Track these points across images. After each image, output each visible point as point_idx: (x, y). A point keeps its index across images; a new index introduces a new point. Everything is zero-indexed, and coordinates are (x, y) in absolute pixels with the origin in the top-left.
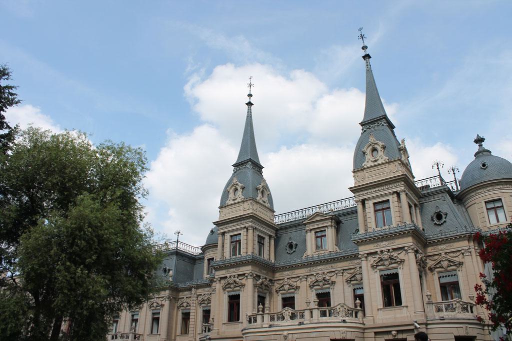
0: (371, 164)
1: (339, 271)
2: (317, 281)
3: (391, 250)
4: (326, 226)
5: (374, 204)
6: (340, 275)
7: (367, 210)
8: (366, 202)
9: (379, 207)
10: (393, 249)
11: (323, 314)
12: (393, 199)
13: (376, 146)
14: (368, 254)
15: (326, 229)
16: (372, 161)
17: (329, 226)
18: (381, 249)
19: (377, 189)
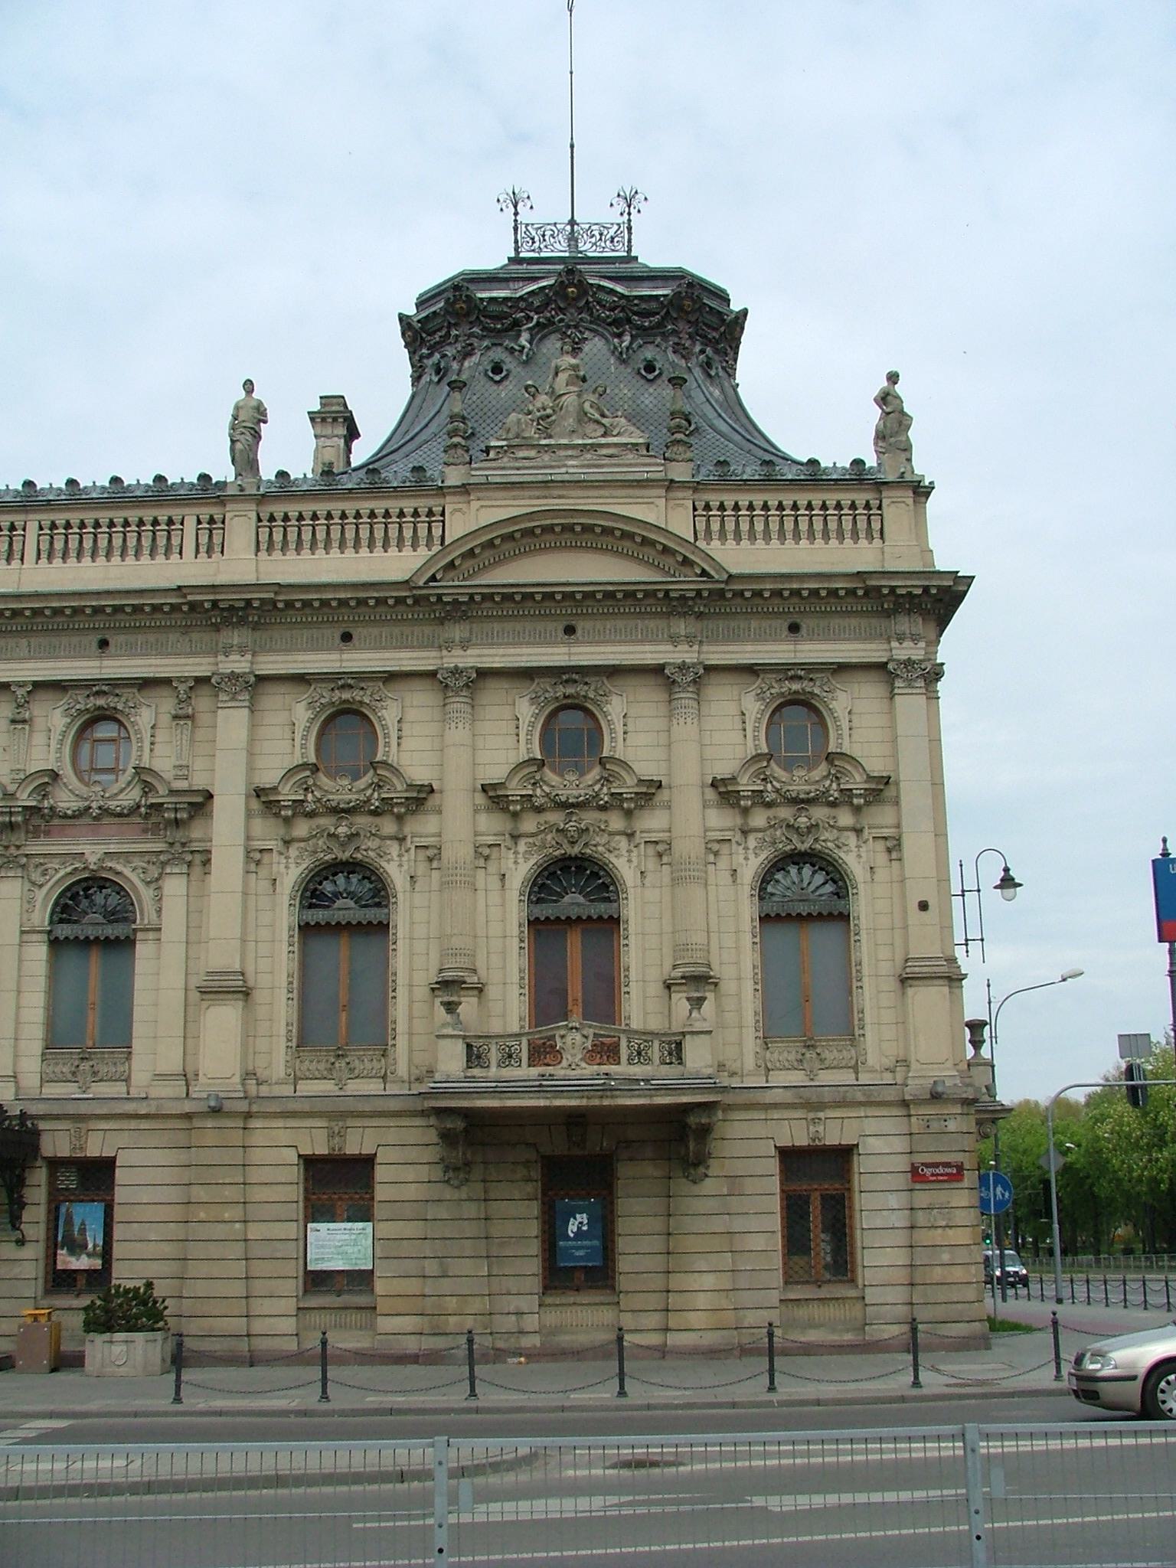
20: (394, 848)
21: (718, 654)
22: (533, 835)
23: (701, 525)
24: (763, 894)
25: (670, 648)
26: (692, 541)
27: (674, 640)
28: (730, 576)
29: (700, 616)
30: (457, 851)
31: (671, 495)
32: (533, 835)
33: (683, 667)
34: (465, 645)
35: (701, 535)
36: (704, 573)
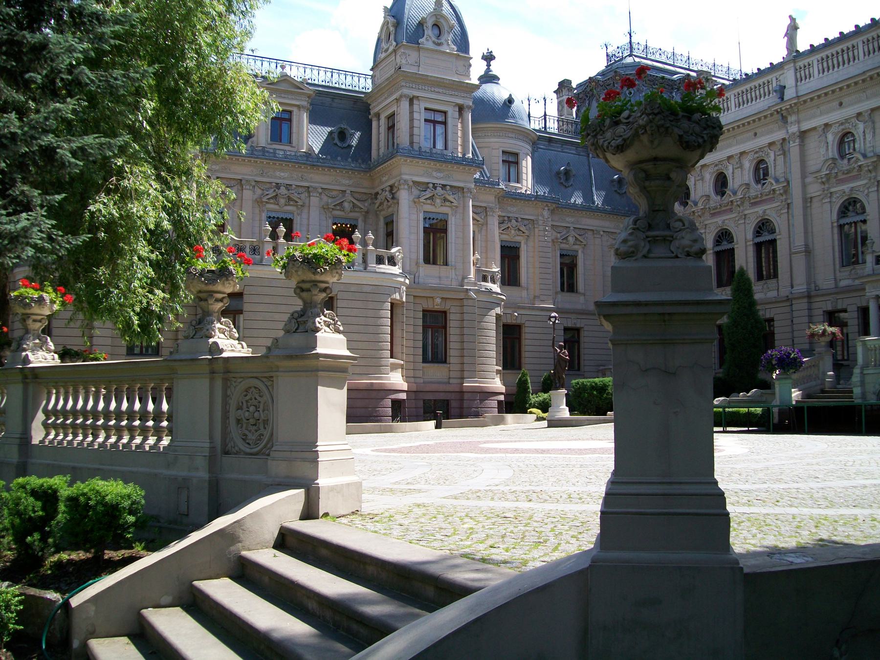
0: (430, 45)
1: (315, 188)
2: (275, 197)
3: (448, 187)
4: (298, 107)
5: (426, 109)
6: (314, 194)
7: (416, 116)
8: (415, 102)
9: (430, 116)
10: (451, 186)
11: (380, 260)
12: (452, 113)
13: (442, 21)
14: (414, 182)
15: (295, 110)
16: (434, 42)
17: (303, 107)
18: (435, 181)
19: (437, 90)
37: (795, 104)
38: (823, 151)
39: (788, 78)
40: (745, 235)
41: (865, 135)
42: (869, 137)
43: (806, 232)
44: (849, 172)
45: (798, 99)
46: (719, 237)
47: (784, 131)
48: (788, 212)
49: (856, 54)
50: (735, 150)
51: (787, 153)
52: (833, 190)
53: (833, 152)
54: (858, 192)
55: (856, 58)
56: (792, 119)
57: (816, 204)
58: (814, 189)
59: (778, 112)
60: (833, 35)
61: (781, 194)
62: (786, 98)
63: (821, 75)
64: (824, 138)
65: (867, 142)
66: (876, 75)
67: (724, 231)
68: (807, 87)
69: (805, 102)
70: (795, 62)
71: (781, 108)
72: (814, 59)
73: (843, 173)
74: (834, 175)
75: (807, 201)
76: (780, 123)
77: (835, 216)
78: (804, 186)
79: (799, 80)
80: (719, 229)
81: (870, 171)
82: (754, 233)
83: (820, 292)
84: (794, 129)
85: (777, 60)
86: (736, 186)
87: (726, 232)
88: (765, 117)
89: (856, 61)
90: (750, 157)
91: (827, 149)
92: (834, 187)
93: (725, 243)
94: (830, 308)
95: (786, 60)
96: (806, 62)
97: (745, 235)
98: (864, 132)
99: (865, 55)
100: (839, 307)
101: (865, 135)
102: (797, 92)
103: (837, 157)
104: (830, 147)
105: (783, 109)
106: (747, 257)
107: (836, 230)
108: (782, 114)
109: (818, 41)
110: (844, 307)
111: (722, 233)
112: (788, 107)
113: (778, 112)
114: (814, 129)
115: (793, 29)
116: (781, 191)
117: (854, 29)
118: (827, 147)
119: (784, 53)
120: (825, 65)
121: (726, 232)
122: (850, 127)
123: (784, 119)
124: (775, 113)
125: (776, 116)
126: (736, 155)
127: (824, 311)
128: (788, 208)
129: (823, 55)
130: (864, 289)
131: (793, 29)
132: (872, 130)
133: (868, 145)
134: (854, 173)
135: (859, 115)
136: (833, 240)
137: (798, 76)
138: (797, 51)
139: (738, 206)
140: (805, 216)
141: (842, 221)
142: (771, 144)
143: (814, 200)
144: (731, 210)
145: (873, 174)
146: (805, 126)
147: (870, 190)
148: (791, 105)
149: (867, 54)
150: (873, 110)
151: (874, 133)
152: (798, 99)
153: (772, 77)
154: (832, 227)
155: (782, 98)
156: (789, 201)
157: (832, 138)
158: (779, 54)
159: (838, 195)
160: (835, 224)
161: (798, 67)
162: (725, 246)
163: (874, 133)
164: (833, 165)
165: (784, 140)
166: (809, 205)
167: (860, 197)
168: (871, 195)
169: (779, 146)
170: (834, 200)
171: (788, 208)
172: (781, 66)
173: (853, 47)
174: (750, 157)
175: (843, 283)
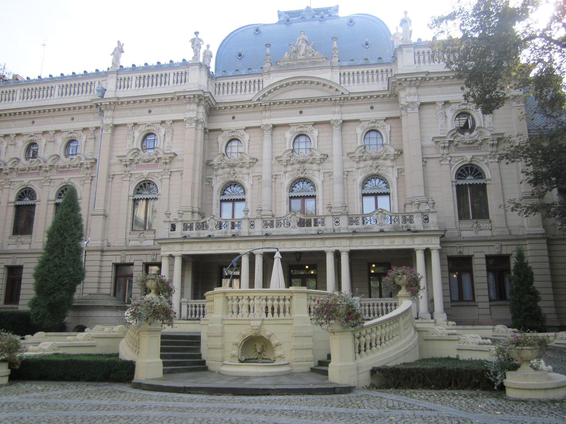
20: (246, 177)
21: (347, 117)
22: (291, 171)
23: (342, 79)
24: (363, 187)
25: (333, 116)
26: (339, 83)
27: (334, 113)
28: (350, 93)
29: (341, 106)
30: (266, 177)
31: (333, 70)
32: (291, 171)
33: (336, 121)
34: (270, 117)
35: (342, 82)
36: (342, 93)
37: (114, 103)
38: (129, 142)
39: (110, 85)
40: (48, 196)
41: (165, 138)
42: (168, 139)
43: (106, 200)
44: (149, 161)
45: (118, 100)
46: (22, 193)
47: (100, 122)
48: (91, 183)
49: (167, 80)
50: (51, 127)
51: (99, 139)
52: (132, 172)
53: (137, 144)
54: (153, 177)
55: (167, 83)
56: (107, 113)
57: (117, 179)
58: (118, 169)
59: (97, 106)
60: (152, 62)
61: (88, 168)
62: (105, 97)
63: (137, 88)
64: (132, 133)
65: (166, 143)
66: (183, 97)
67: (28, 190)
68: (122, 93)
69: (122, 103)
70: (118, 74)
71: (101, 103)
72: (134, 76)
73: (144, 161)
74: (136, 161)
75: (111, 177)
76: (97, 115)
77: (131, 193)
78: (110, 165)
79: (119, 87)
80: (24, 187)
81: (166, 163)
82: (56, 196)
83: (111, 248)
84: (108, 121)
85: (103, 68)
86: (46, 156)
87: (30, 191)
88: (85, 107)
89: (167, 85)
90: (65, 135)
91: (133, 142)
92: (134, 170)
93: (28, 199)
94: (119, 261)
95: (110, 70)
96: (126, 76)
97: (48, 196)
98: (165, 135)
99: (174, 83)
100: (127, 261)
101: (165, 138)
102: (115, 95)
103: (140, 148)
104: (135, 141)
105: (103, 104)
106: (47, 213)
107: (131, 203)
108: (100, 108)
109: (140, 63)
110: (132, 261)
111: (26, 191)
112: (107, 103)
113: (97, 106)
114: (125, 125)
115: (119, 50)
116: (89, 166)
117: (169, 63)
118: (134, 140)
119: (110, 65)
120: (142, 82)
121: (30, 191)
122: (155, 129)
123: (102, 112)
124: (95, 106)
125: (94, 108)
126: (52, 131)
127: (113, 264)
128: (92, 180)
129: (142, 75)
130: (160, 249)
131: (119, 50)
132: (171, 135)
133: (166, 145)
134: (153, 163)
135: (163, 122)
136: (128, 209)
137: (119, 85)
138: (121, 67)
139: (47, 171)
140: (107, 187)
141: (137, 197)
142: (85, 129)
143: (115, 177)
144: (38, 174)
145: (168, 166)
146: (117, 122)
147: (163, 177)
148: (110, 102)
149: (175, 82)
150: (174, 121)
151: (172, 137)
152: (118, 100)
153: (96, 81)
154: (129, 200)
155: (102, 97)
156: (93, 175)
157: (138, 134)
158: (105, 64)
159: (136, 176)
160: (131, 198)
161: (119, 78)
162: (27, 201)
163: (172, 137)
164: (137, 154)
165: (97, 128)
166: (111, 180)
167: (156, 181)
168: (163, 181)
169: (92, 132)
170: (132, 179)
171: (92, 180)
172: (106, 74)
173: (166, 75)
174: (65, 135)
175: (132, 243)
